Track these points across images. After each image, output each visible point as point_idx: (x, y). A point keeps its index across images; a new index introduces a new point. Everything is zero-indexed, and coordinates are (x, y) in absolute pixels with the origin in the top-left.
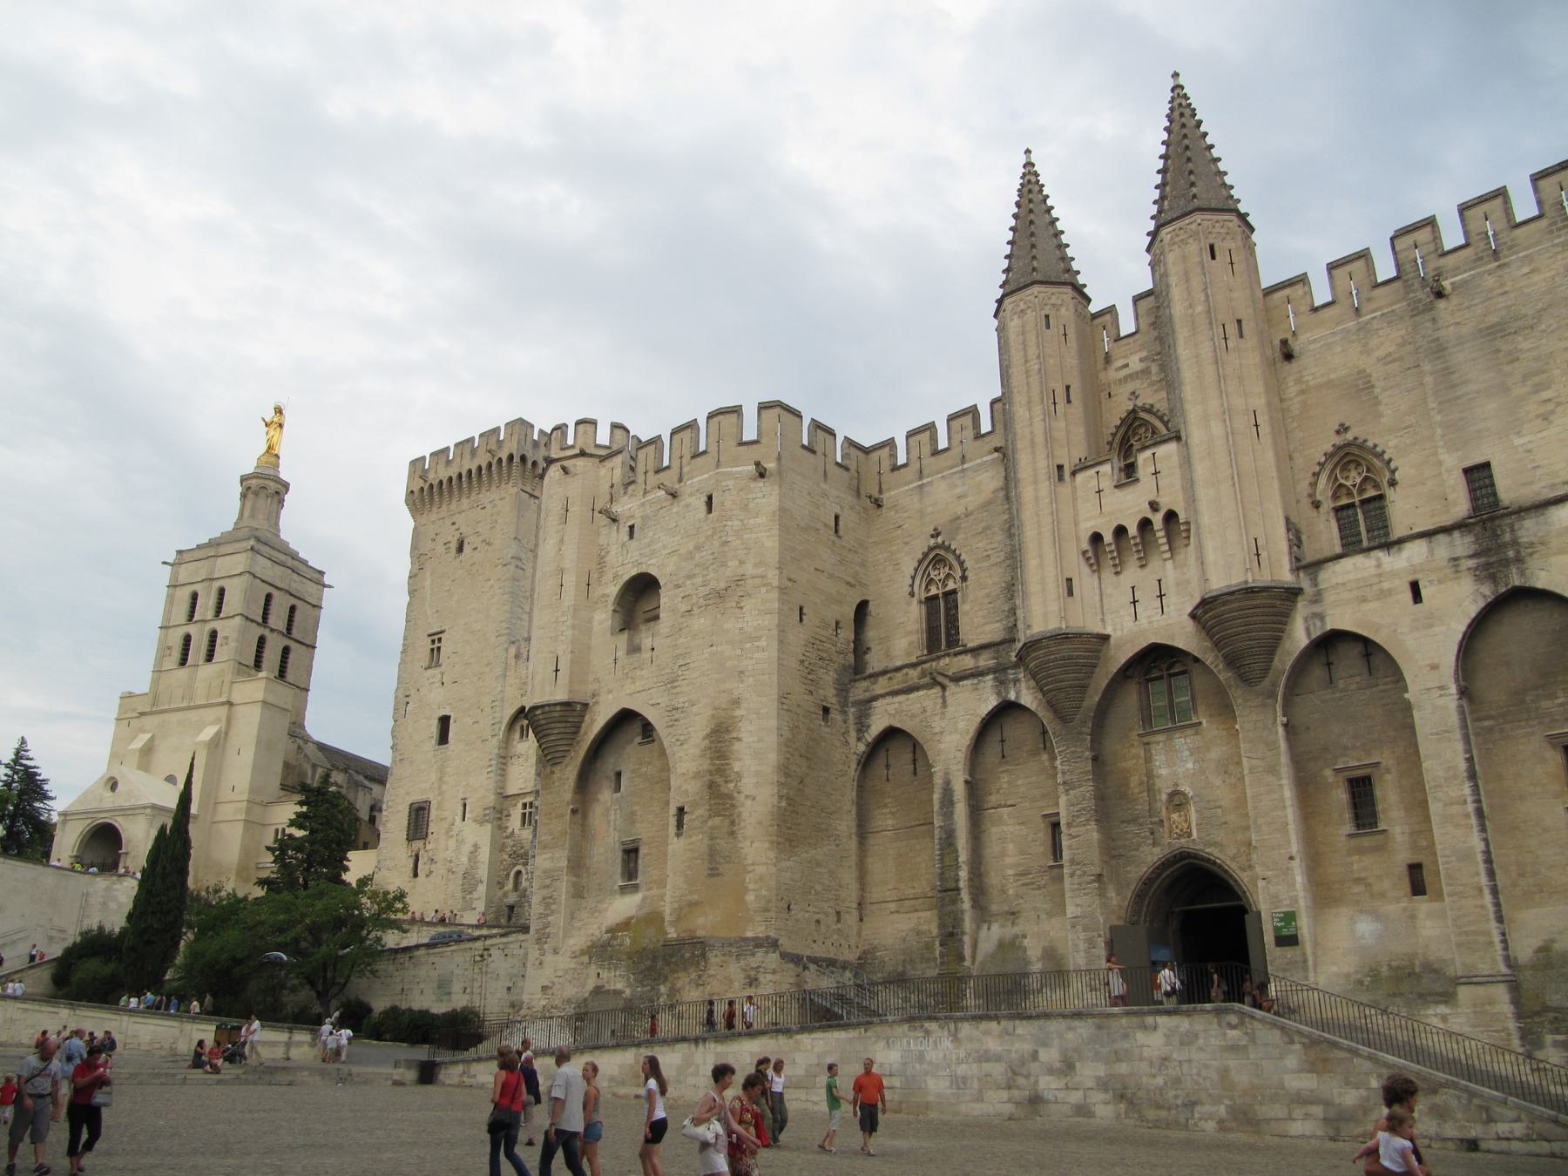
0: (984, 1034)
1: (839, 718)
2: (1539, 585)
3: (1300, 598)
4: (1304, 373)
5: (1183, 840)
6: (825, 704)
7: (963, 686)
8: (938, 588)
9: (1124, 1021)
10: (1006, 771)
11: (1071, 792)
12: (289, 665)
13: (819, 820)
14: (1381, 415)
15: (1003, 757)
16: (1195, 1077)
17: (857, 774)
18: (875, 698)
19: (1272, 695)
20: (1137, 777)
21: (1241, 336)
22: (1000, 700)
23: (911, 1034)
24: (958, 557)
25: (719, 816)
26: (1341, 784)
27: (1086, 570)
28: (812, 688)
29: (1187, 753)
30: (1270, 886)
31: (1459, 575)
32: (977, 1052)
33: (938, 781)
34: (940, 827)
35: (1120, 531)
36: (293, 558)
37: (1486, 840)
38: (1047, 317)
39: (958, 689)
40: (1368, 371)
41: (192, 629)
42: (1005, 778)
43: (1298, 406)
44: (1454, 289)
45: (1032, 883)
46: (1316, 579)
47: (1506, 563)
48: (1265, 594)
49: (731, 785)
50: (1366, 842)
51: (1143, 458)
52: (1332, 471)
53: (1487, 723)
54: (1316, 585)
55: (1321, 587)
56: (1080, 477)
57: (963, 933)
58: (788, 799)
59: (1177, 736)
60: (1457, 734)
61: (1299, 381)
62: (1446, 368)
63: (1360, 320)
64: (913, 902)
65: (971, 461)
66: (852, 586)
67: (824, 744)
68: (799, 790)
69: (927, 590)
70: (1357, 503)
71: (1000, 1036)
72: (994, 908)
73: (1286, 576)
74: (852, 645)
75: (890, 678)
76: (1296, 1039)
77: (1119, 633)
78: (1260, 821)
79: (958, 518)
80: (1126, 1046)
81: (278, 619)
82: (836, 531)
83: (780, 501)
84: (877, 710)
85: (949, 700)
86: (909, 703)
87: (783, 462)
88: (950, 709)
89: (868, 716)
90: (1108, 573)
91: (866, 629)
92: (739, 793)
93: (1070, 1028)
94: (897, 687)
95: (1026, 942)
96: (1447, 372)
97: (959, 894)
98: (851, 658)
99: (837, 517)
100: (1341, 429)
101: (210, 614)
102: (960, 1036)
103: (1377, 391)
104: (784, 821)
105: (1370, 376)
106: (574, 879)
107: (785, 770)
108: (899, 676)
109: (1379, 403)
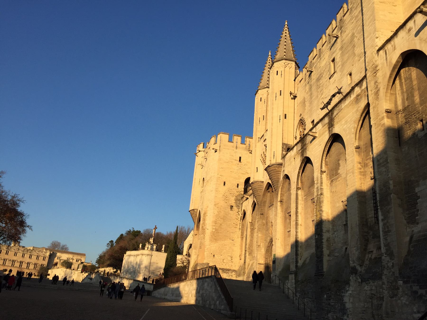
1: (236, 208)
2: (307, 156)
6: (231, 205)
17: (241, 222)
25: (202, 234)
27: (262, 164)
37: (296, 232)
49: (205, 227)
52: (299, 127)
58: (216, 229)
67: (230, 215)
68: (220, 227)
73: (280, 161)
83: (219, 157)
92: (206, 228)
99: (240, 158)
100: (301, 115)
104: (214, 235)
106: (195, 251)
107: (215, 222)
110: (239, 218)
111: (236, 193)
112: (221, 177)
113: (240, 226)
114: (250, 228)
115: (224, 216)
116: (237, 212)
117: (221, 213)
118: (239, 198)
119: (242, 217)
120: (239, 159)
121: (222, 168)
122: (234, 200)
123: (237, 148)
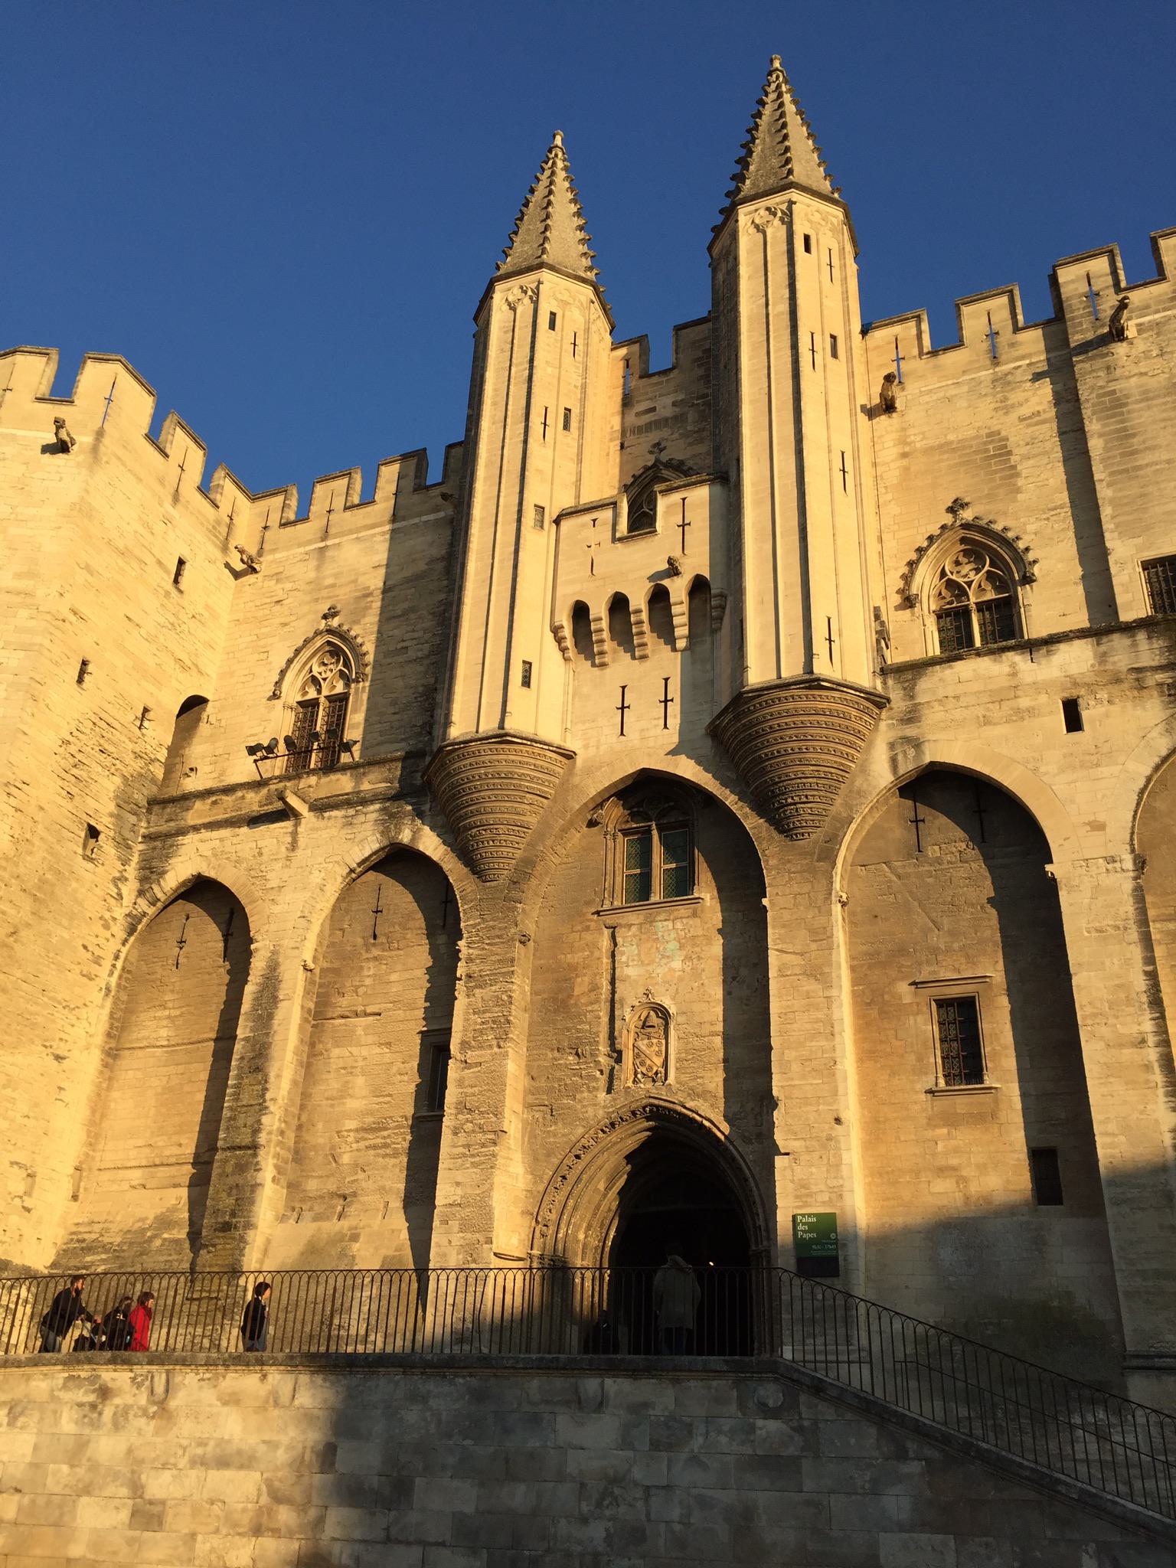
0: (225, 1403)
1: (113, 851)
3: (884, 714)
4: (911, 432)
5: (649, 1085)
6: (93, 823)
7: (329, 818)
8: (319, 692)
9: (535, 1385)
10: (375, 958)
11: (477, 991)
13: (34, 1009)
14: (1018, 491)
15: (375, 937)
16: (677, 1527)
17: (125, 950)
18: (182, 832)
20: (586, 979)
21: (835, 355)
22: (386, 843)
23: (66, 1396)
26: (925, 1009)
28: (74, 791)
29: (673, 945)
30: (798, 1169)
31: (1145, 693)
32: (202, 1443)
33: (258, 965)
34: (243, 1039)
35: (619, 604)
39: (322, 824)
40: (1003, 433)
42: (370, 969)
43: (897, 473)
44: (1140, 332)
45: (386, 1146)
46: (913, 689)
48: (836, 694)
50: (963, 1102)
51: (665, 505)
54: (912, 697)
55: (921, 699)
56: (565, 525)
57: (249, 1225)
59: (662, 917)
60: (1134, 934)
61: (903, 441)
62: (1125, 429)
63: (997, 369)
64: (172, 1170)
65: (404, 519)
66: (184, 668)
67: (74, 885)
69: (305, 693)
70: (973, 607)
71: (262, 1409)
72: (312, 1186)
74: (165, 752)
75: (215, 803)
76: (912, 1446)
77: (592, 751)
78: (790, 1055)
79: (370, 594)
80: (534, 1443)
82: (176, 581)
84: (183, 850)
85: (302, 841)
86: (235, 840)
87: (106, 440)
88: (299, 852)
89: (168, 857)
91: (196, 740)
93: (414, 1397)
94: (220, 817)
95: (356, 1246)
96: (1124, 435)
97: (255, 1155)
98: (159, 773)
99: (181, 563)
102: (173, 1404)
103: (1014, 459)
105: (1008, 439)
108: (228, 800)
109: (1018, 475)
110: (114, 919)
111: (129, 758)
112: (73, 618)
113: (111, 974)
114: (302, 1007)
115: (43, 881)
116: (116, 881)
117: (30, 853)
118: (136, 796)
119: (145, 920)
121: (88, 568)
122: (112, 795)
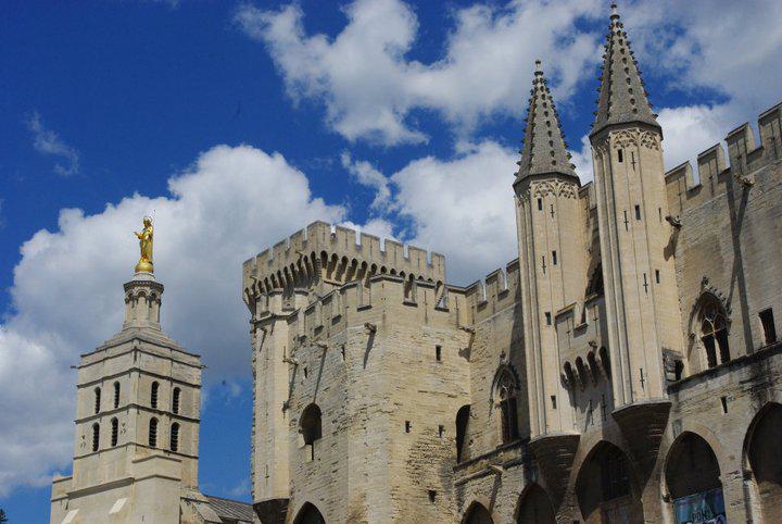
12: (179, 439)
18: (465, 482)
19: (658, 478)
24: (515, 372)
29: (625, 517)
35: (579, 361)
36: (172, 349)
38: (540, 201)
41: (97, 421)
47: (764, 386)
53: (766, 495)
81: (164, 403)
87: (388, 319)
90: (578, 391)
96: (752, 241)
99: (438, 349)
100: (705, 281)
101: (112, 408)
112: (397, 407)
120: (435, 354)
123: (426, 319)
